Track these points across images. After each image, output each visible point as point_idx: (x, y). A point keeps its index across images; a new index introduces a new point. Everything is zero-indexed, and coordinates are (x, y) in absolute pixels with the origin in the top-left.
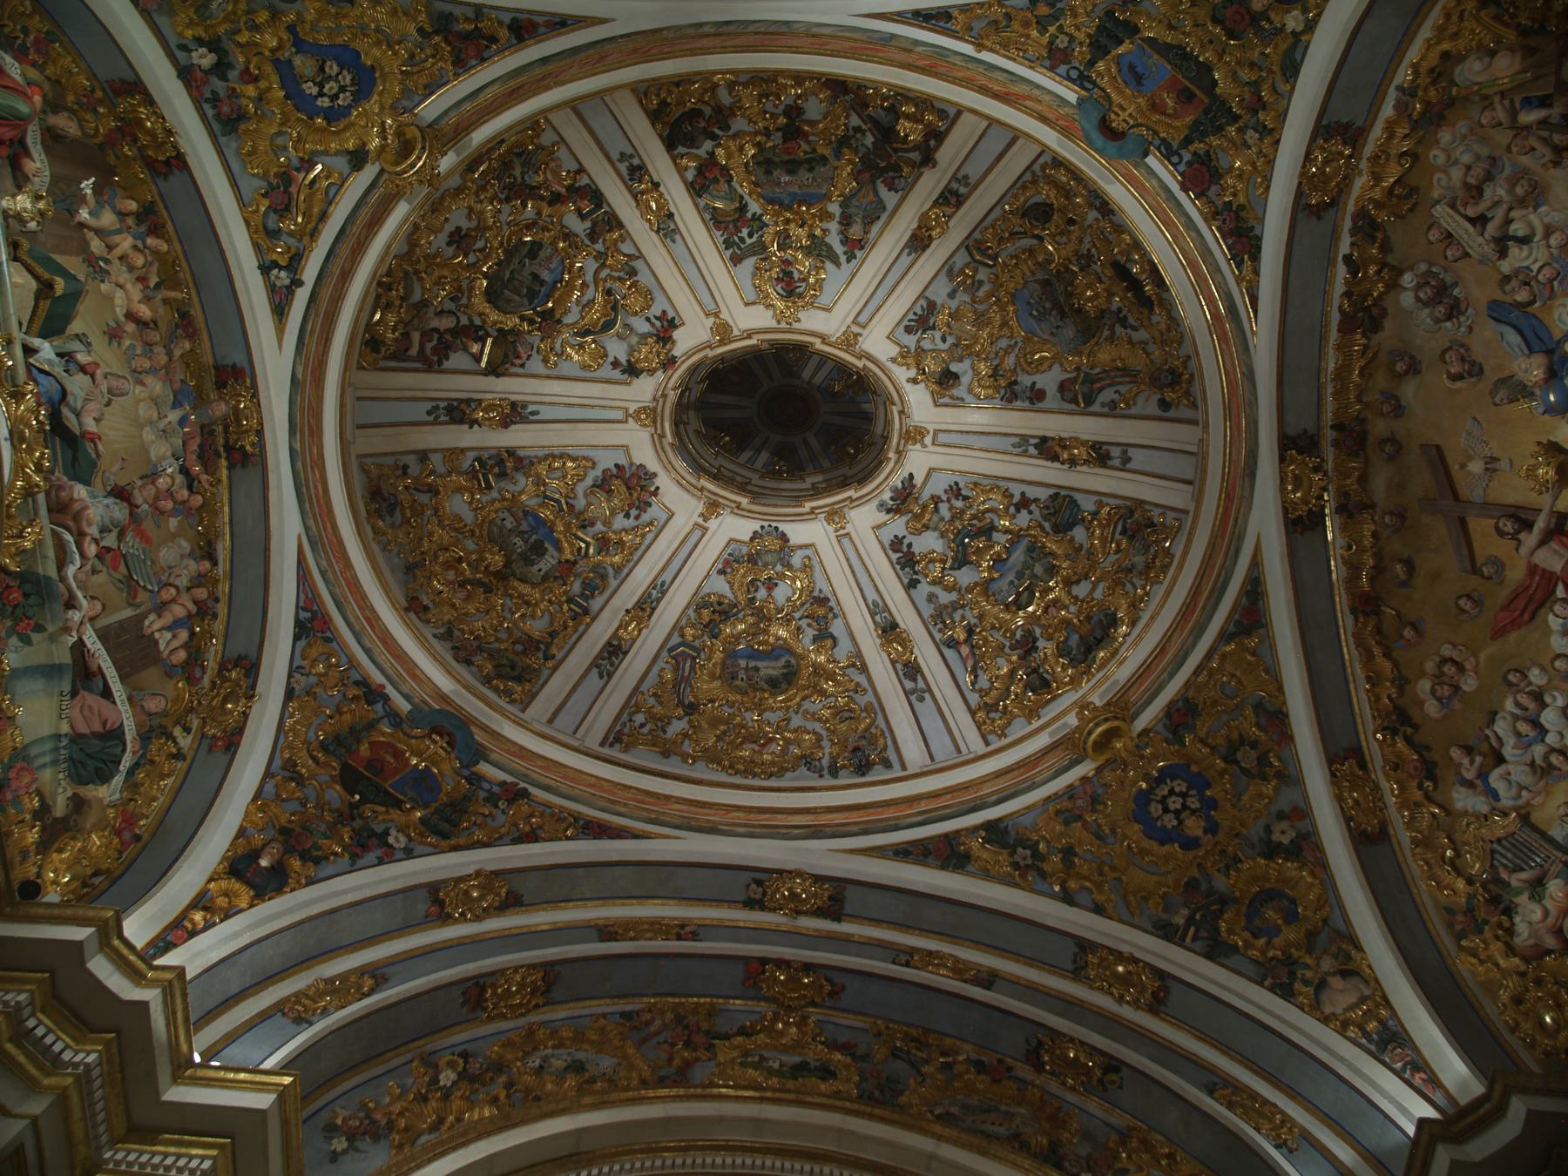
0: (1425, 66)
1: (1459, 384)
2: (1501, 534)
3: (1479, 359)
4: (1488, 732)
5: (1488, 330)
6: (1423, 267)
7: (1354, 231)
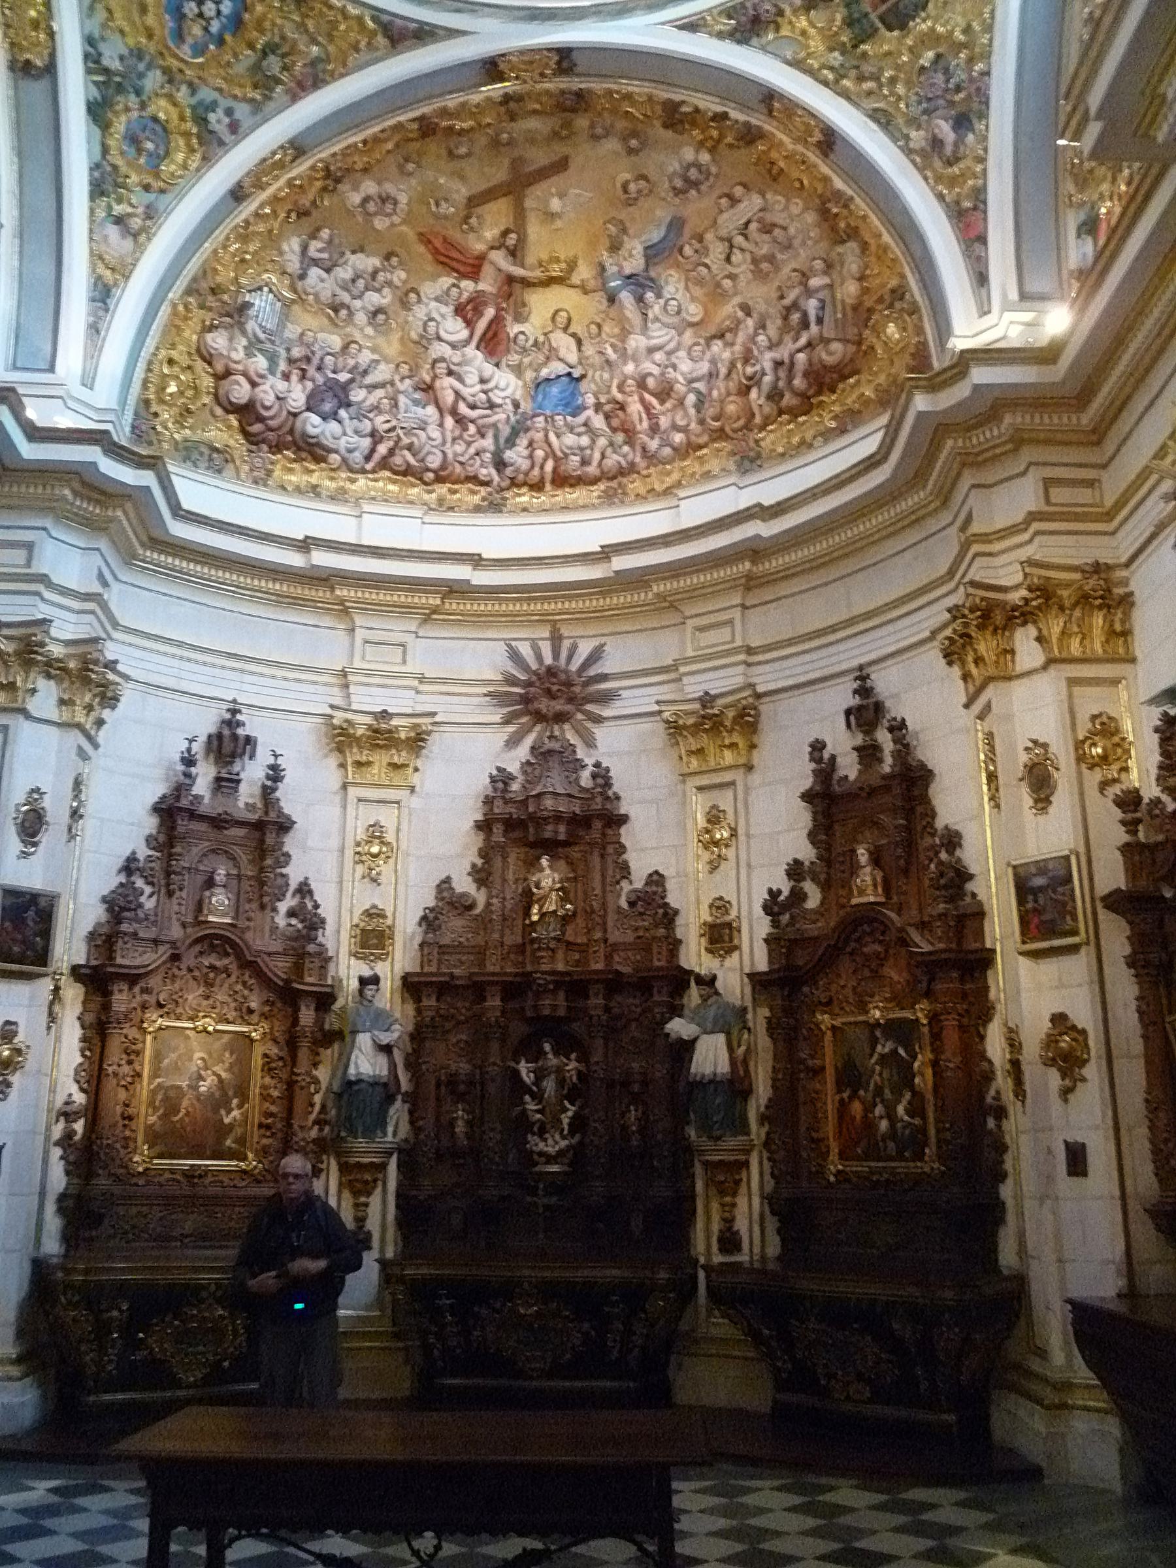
0: (862, 226)
1: (619, 185)
2: (505, 233)
3: (640, 203)
4: (348, 253)
5: (663, 214)
6: (714, 170)
7: (747, 124)
